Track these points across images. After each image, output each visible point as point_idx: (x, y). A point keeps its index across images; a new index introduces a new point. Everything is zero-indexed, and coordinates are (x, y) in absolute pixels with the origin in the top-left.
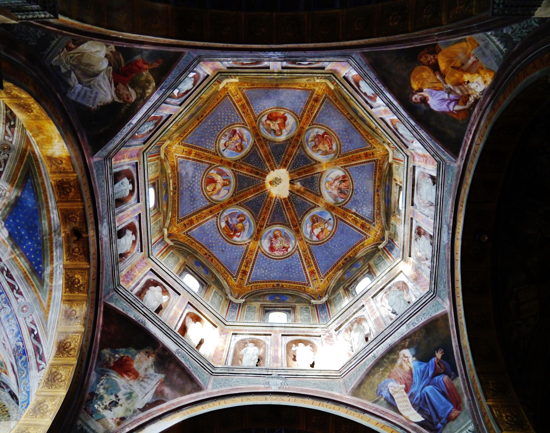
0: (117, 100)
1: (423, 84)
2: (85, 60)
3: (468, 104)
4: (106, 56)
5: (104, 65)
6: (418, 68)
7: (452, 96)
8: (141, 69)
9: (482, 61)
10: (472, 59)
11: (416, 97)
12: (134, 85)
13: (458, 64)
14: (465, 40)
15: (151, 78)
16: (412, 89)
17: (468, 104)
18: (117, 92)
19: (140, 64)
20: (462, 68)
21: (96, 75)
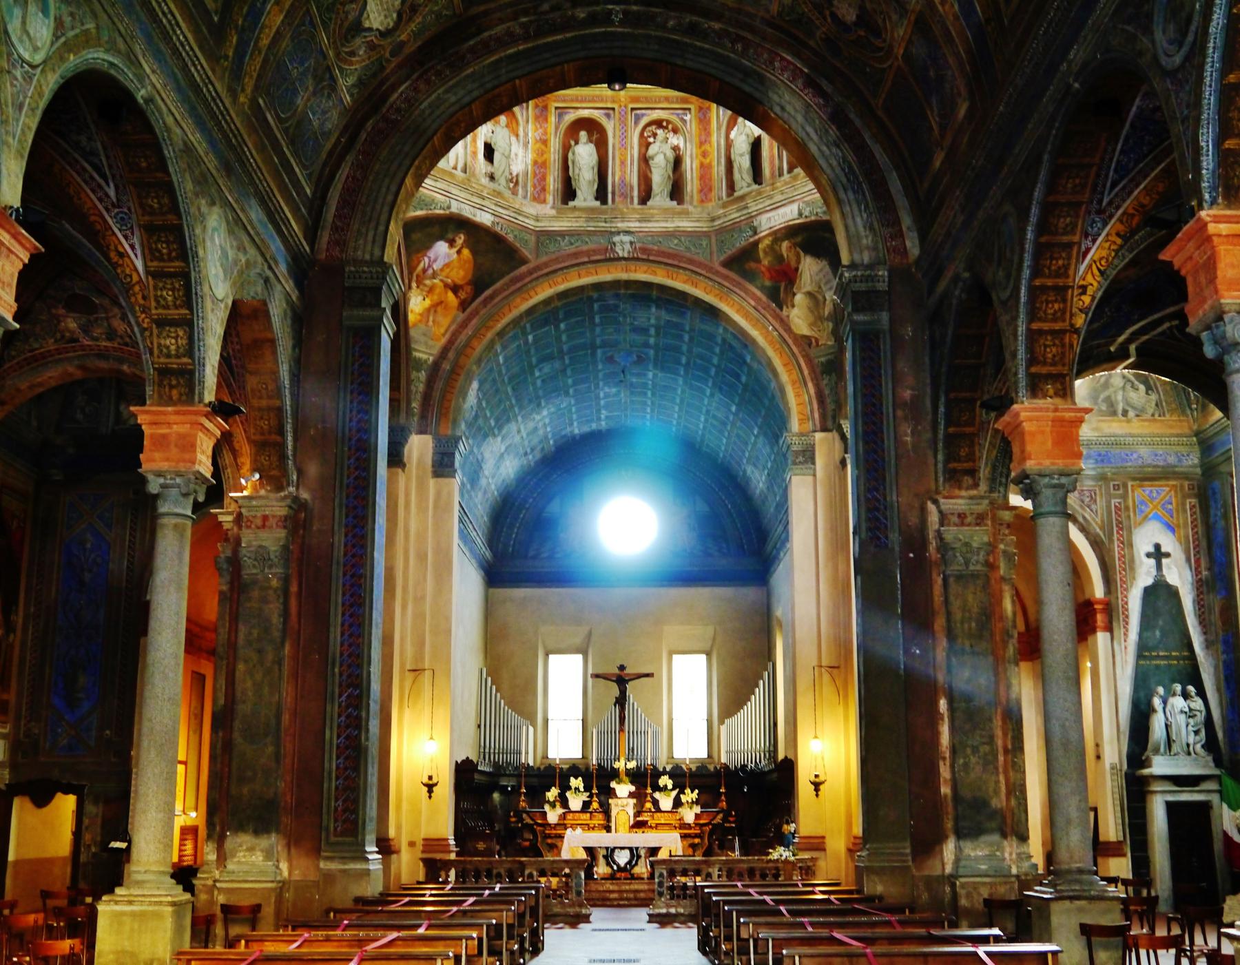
0: (802, 254)
1: (459, 259)
2: (812, 319)
3: (415, 278)
4: (793, 306)
5: (799, 298)
6: (470, 277)
7: (430, 271)
8: (769, 270)
9: (422, 326)
10: (431, 323)
11: (460, 239)
12: (780, 258)
13: (439, 309)
14: (444, 335)
15: (761, 254)
16: (468, 247)
17: (415, 278)
18: (798, 262)
19: (767, 274)
20: (434, 307)
21: (809, 294)
